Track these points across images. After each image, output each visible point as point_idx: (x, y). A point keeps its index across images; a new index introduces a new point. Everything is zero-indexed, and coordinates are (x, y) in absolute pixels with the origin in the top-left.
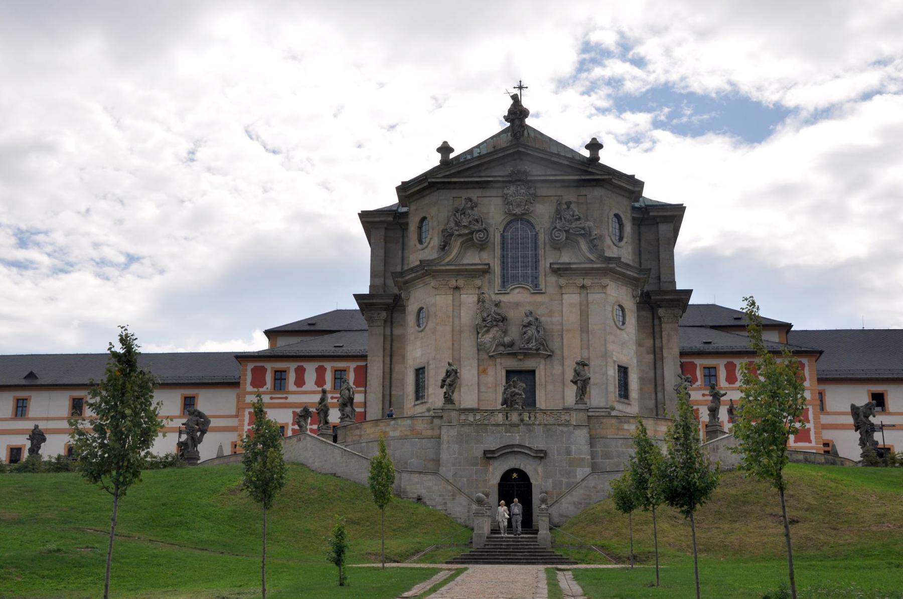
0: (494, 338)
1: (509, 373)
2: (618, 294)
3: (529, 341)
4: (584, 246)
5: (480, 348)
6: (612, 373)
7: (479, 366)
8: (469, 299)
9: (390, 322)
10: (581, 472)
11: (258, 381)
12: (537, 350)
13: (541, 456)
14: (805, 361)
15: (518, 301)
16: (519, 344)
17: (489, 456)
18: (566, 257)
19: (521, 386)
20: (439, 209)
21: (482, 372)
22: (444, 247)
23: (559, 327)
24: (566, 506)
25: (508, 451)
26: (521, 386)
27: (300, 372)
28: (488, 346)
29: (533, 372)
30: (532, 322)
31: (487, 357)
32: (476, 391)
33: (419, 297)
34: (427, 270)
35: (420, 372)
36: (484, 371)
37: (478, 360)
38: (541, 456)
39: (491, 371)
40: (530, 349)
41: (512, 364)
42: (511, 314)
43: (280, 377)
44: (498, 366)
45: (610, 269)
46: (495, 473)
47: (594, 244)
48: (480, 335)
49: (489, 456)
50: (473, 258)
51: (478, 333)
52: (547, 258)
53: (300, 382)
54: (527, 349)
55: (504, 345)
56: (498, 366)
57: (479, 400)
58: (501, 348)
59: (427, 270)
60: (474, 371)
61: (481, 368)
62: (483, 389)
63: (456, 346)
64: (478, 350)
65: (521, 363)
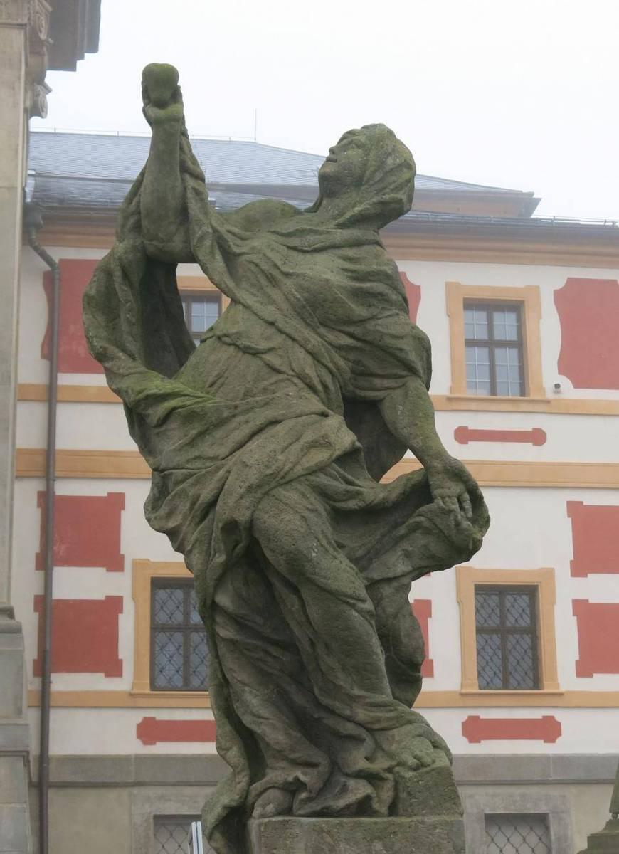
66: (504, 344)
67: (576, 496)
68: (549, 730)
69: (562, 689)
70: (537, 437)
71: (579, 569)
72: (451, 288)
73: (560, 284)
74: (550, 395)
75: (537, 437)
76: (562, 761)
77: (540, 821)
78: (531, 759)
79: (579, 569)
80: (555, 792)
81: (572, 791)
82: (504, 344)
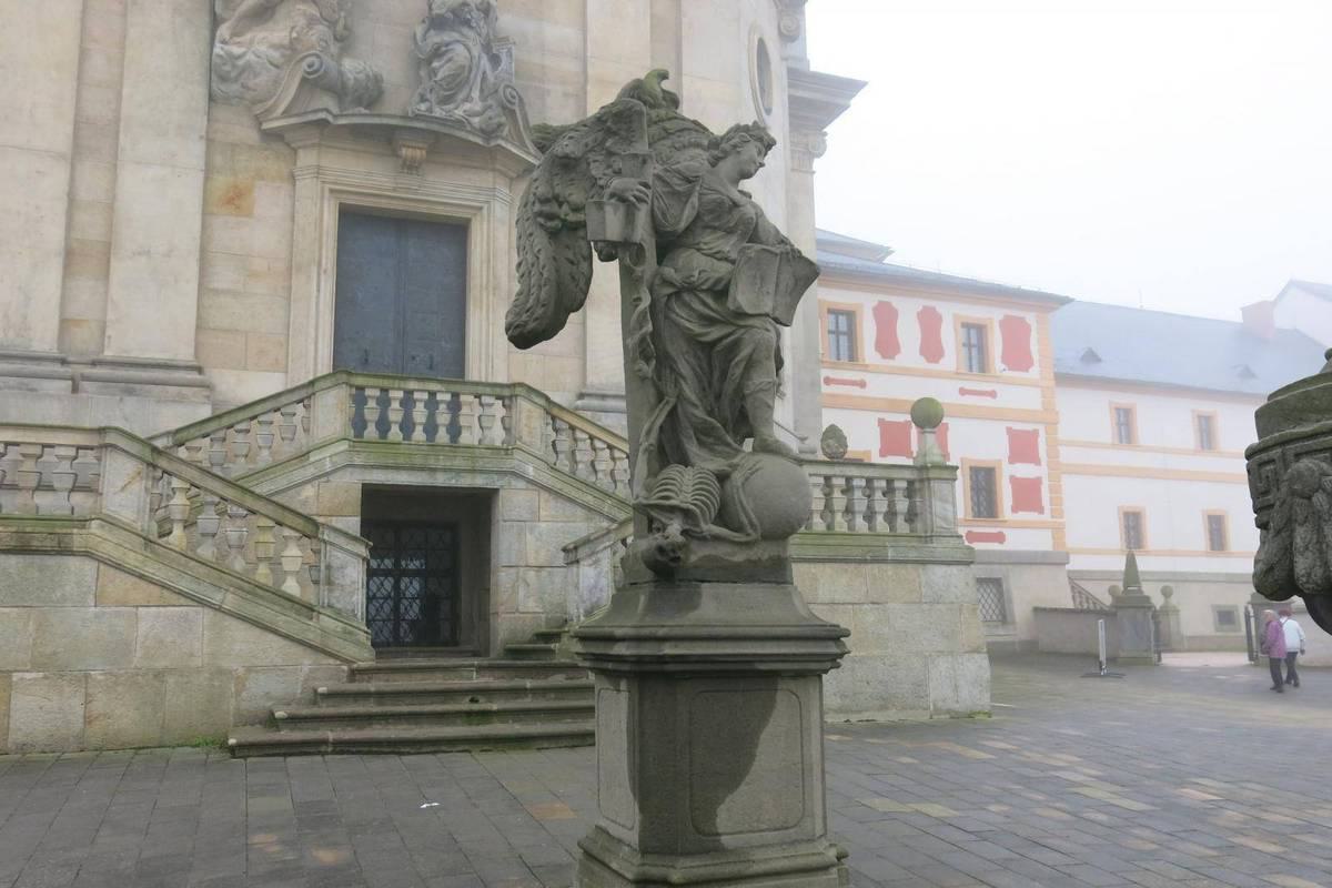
0: (292, 49)
1: (353, 219)
3: (454, 87)
5: (222, 85)
7: (209, 171)
12: (488, 134)
14: (1031, 318)
16: (398, 102)
21: (225, 202)
23: (571, 67)
28: (262, 81)
31: (252, 136)
32: (192, 288)
36: (236, 200)
37: (210, 141)
39: (269, 202)
40: (459, 124)
41: (371, 178)
44: (307, 186)
48: (224, 31)
51: (216, 21)
54: (442, 121)
55: (338, 90)
56: (307, 186)
57: (200, 327)
58: (327, 101)
60: (187, 192)
61: (221, 181)
62: (224, 277)
63: (98, 65)
64: (211, 98)
65: (410, 181)
66: (974, 346)
67: (1010, 424)
68: (1000, 538)
69: (1006, 518)
70: (993, 394)
71: (1013, 459)
72: (956, 317)
73: (1001, 317)
74: (998, 374)
75: (993, 394)
76: (1009, 554)
77: (997, 582)
78: (994, 552)
79: (1013, 459)
80: (1003, 567)
81: (1010, 567)
82: (974, 346)
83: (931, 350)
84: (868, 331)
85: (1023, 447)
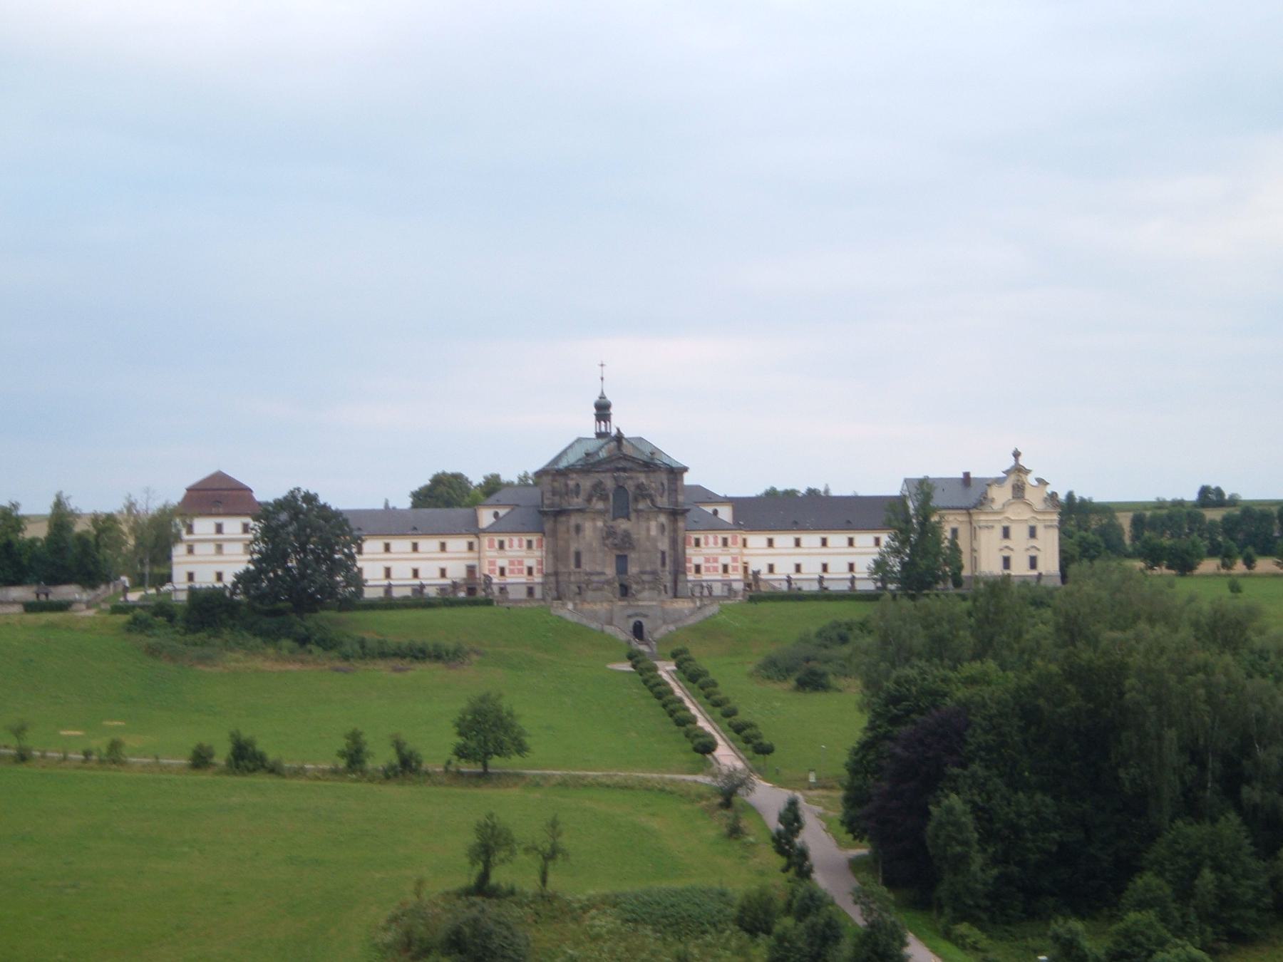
2: (663, 519)
4: (648, 502)
6: (659, 555)
8: (600, 524)
9: (555, 521)
10: (660, 622)
11: (491, 546)
13: (645, 616)
15: (623, 525)
17: (629, 617)
18: (641, 506)
19: (622, 561)
20: (587, 483)
22: (589, 500)
24: (657, 635)
25: (636, 615)
26: (622, 561)
27: (511, 541)
29: (625, 556)
30: (627, 535)
33: (574, 520)
34: (579, 511)
35: (578, 555)
38: (645, 616)
41: (619, 553)
42: (618, 530)
43: (501, 545)
45: (661, 510)
46: (632, 622)
47: (653, 501)
49: (629, 617)
50: (600, 506)
52: (632, 506)
53: (511, 546)
59: (579, 511)
83: (716, 543)
84: (702, 541)
85: (735, 560)
